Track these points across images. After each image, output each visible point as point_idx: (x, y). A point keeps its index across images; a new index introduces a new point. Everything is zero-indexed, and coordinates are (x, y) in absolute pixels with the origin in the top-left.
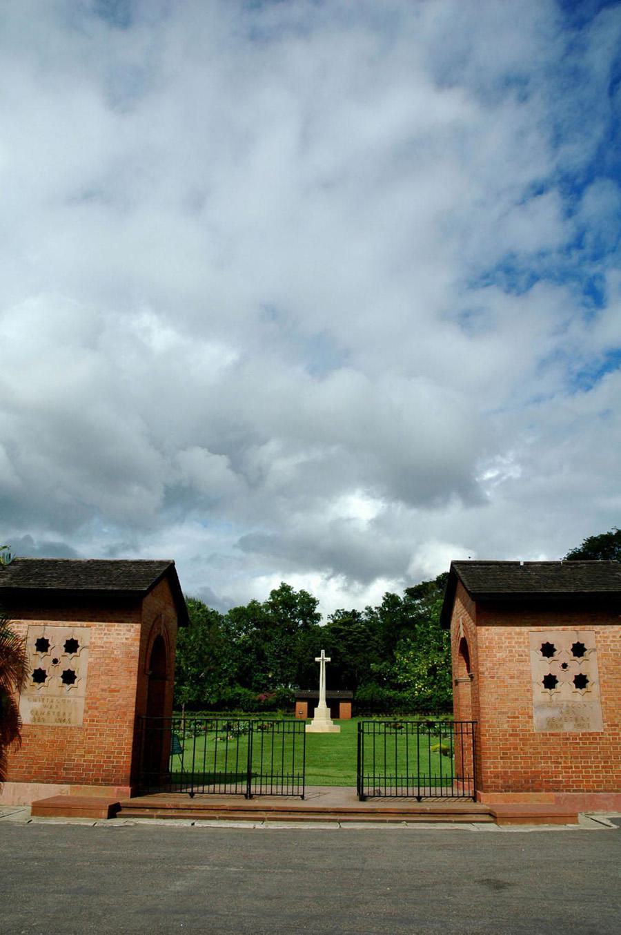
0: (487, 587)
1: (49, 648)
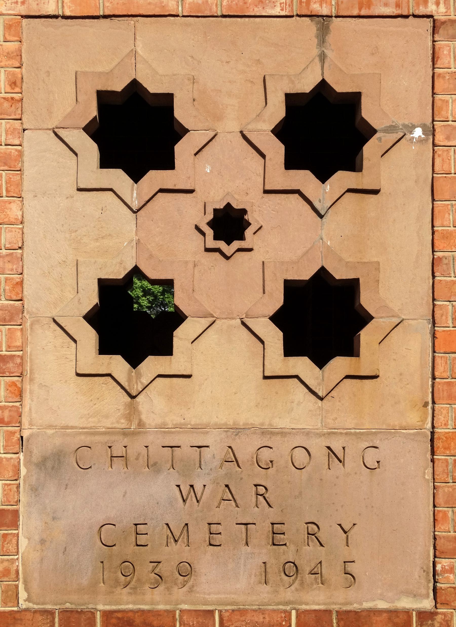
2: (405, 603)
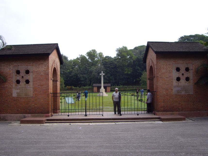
0: (160, 50)
1: (20, 73)
2: (192, 94)
